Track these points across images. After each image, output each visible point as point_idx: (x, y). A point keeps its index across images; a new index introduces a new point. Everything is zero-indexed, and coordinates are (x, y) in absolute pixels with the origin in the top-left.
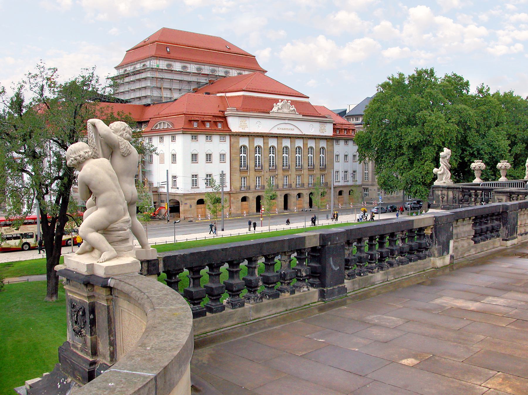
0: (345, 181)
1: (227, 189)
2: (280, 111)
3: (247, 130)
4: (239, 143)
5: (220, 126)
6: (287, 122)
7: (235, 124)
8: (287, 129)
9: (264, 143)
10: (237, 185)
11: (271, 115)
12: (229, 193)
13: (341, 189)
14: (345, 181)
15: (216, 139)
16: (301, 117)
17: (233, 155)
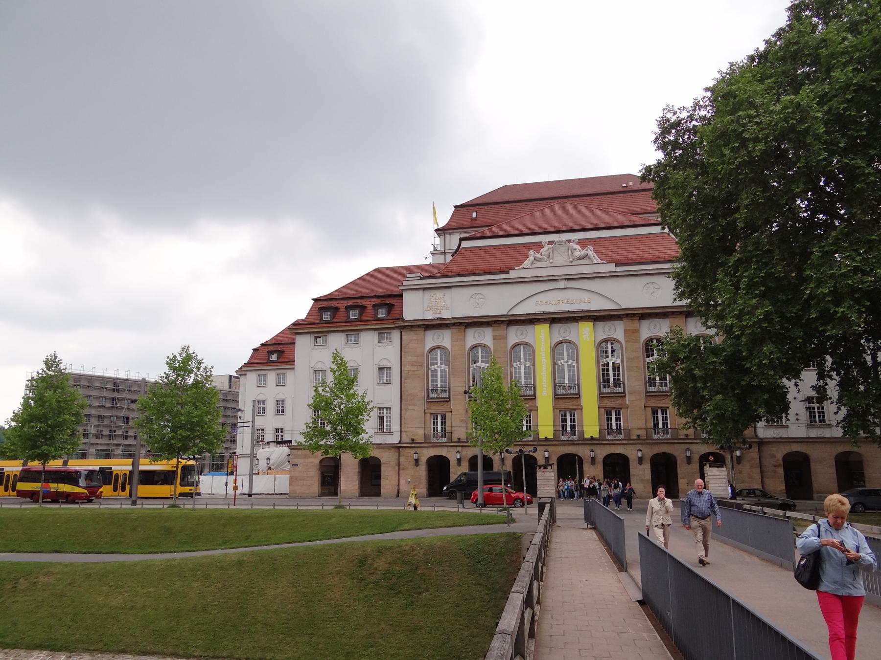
0: (809, 426)
1: (394, 439)
2: (539, 264)
3: (446, 315)
4: (424, 342)
5: (382, 313)
6: (562, 284)
7: (414, 307)
8: (568, 302)
9: (494, 338)
10: (418, 429)
11: (513, 274)
12: (397, 448)
13: (795, 448)
14: (809, 426)
15: (368, 339)
16: (611, 267)
17: (406, 368)
